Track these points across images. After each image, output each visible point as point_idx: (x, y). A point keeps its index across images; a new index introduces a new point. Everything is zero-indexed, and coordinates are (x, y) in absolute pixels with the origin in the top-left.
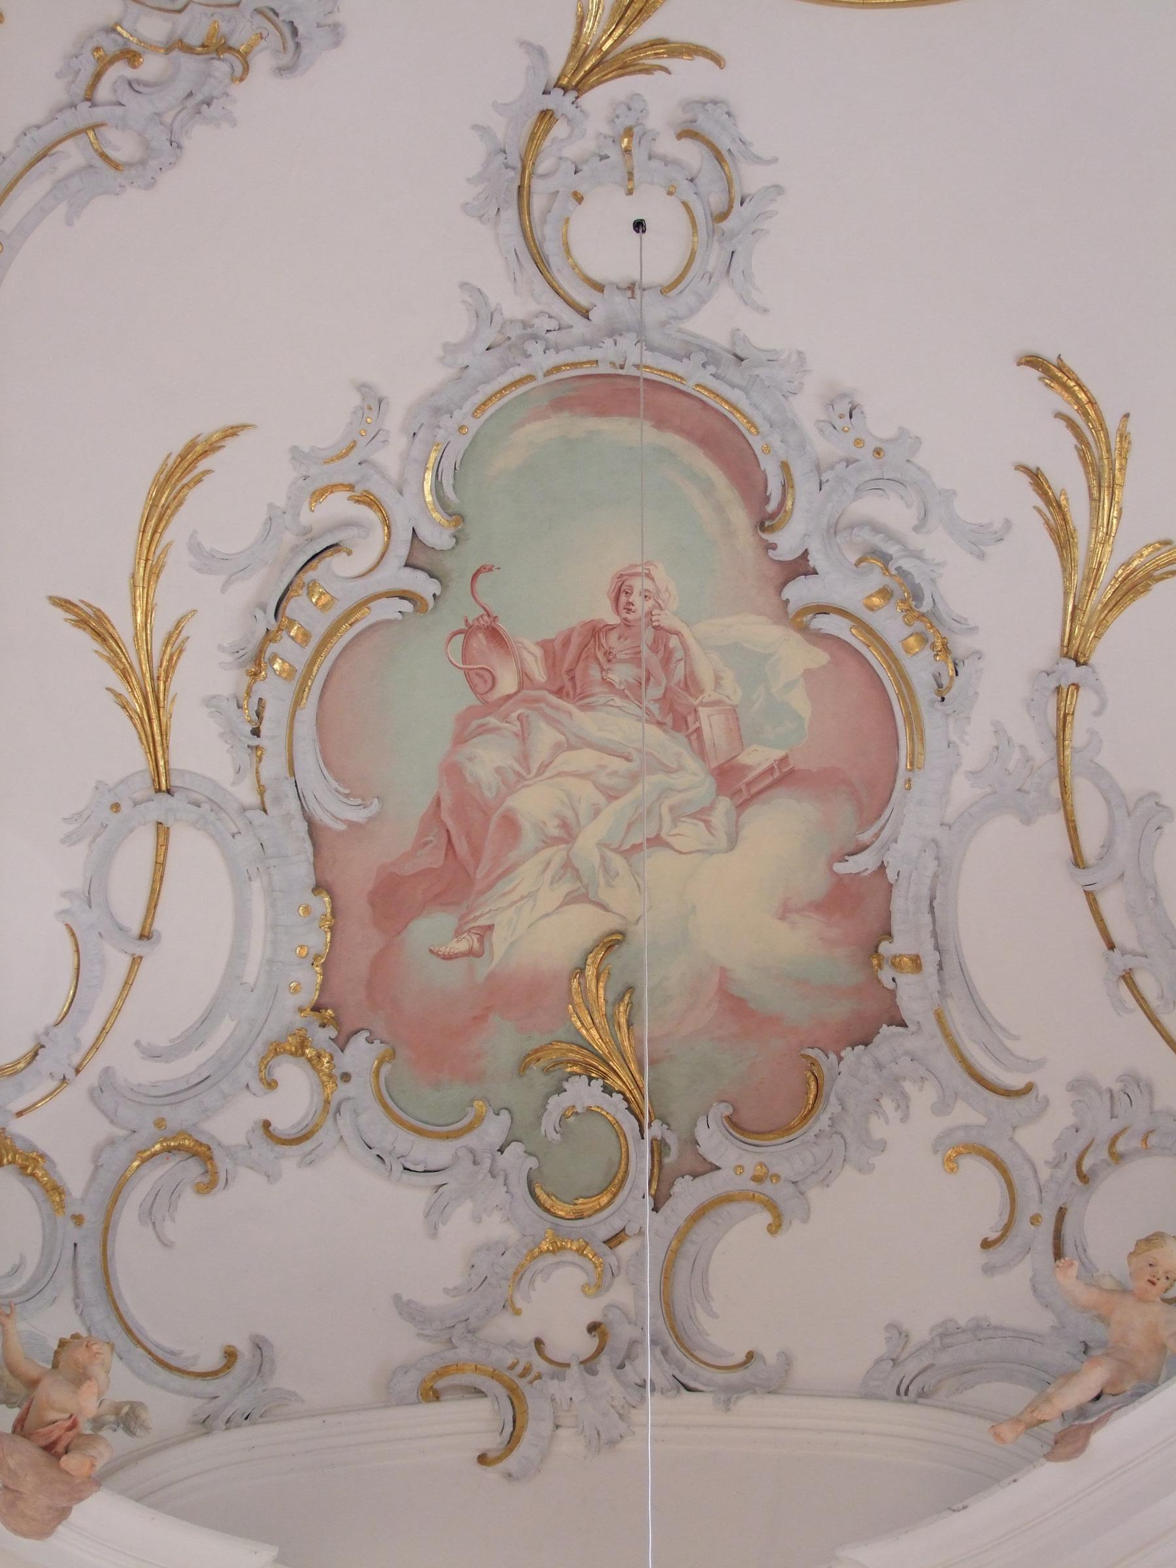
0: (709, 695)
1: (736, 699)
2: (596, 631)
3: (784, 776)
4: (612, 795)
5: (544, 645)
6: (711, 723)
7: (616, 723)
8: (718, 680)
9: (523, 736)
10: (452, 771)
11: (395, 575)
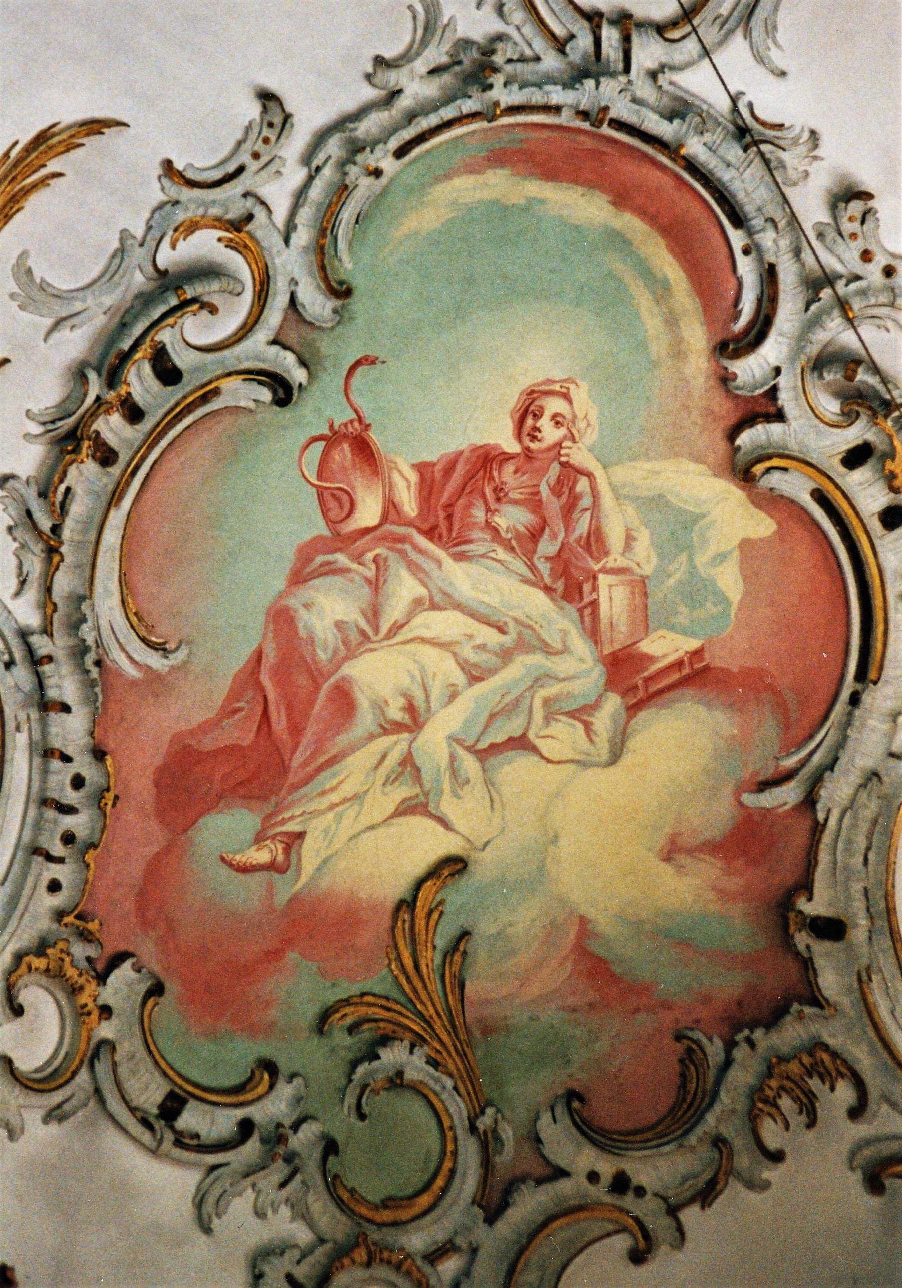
0: (615, 559)
1: (648, 569)
2: (487, 460)
3: (695, 675)
4: (474, 679)
5: (422, 468)
6: (613, 599)
7: (490, 581)
8: (630, 539)
9: (376, 584)
10: (281, 619)
11: (258, 348)
